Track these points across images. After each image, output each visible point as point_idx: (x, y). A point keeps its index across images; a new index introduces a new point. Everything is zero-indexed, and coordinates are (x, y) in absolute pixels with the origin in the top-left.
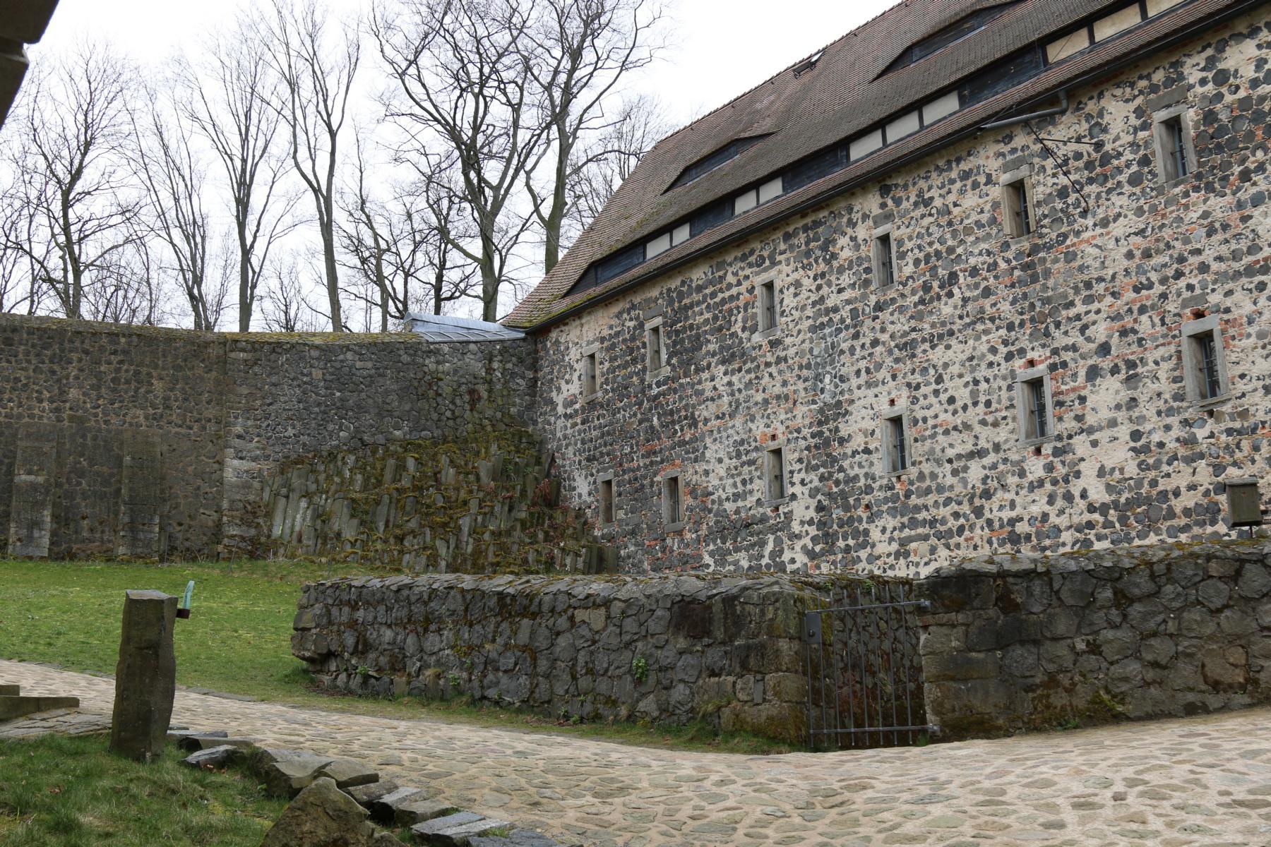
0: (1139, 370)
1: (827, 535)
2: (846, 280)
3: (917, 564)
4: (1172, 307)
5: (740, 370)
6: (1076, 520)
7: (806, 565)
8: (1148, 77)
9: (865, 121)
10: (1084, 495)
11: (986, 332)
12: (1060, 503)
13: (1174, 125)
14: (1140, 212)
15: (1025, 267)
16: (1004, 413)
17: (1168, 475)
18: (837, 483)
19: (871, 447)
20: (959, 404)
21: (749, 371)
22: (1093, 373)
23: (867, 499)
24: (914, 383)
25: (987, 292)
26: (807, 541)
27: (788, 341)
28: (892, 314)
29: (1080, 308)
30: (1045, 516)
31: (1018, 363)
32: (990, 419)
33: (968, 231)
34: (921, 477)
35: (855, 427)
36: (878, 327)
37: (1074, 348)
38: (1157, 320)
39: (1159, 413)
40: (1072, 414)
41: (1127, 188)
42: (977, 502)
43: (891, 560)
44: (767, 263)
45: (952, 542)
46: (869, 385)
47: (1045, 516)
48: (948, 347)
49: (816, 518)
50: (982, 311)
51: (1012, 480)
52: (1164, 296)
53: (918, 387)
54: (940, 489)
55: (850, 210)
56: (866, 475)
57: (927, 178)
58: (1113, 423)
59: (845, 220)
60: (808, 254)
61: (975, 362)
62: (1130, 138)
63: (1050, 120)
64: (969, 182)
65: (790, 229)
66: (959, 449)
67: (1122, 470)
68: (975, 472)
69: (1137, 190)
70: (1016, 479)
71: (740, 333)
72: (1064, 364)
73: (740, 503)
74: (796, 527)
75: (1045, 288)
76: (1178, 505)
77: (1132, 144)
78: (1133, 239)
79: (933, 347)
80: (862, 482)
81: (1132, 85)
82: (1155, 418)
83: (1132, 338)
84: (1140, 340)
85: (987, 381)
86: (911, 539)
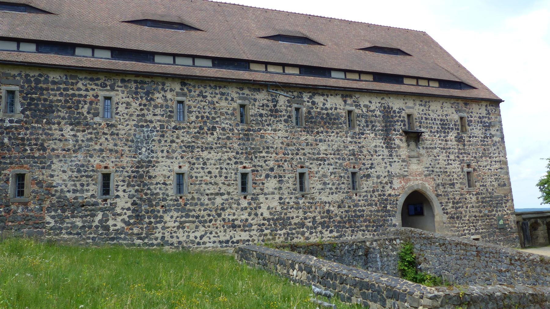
0: (283, 179)
1: (138, 216)
2: (158, 111)
3: (189, 232)
5: (84, 131)
6: (259, 222)
7: (123, 228)
9: (170, 51)
10: (262, 215)
11: (227, 152)
12: (252, 216)
14: (287, 131)
15: (245, 135)
16: (233, 182)
17: (290, 212)
18: (146, 194)
19: (168, 183)
20: (213, 175)
21: (91, 133)
22: (267, 176)
23: (163, 203)
24: (192, 162)
25: (228, 138)
26: (125, 217)
27: (119, 127)
28: (183, 133)
29: (264, 154)
30: (247, 220)
31: (240, 166)
32: (226, 183)
33: (222, 114)
34: (193, 198)
35: (160, 173)
36: (175, 136)
37: (261, 166)
38: (290, 165)
40: (259, 188)
42: (219, 212)
43: (175, 229)
44: (108, 88)
45: (206, 225)
46: (167, 157)
47: (247, 220)
48: (210, 153)
49: (132, 207)
50: (226, 144)
51: (235, 206)
52: (292, 159)
53: (194, 164)
54: (202, 204)
55: (164, 84)
56: (163, 194)
57: (205, 88)
58: (273, 193)
59: (160, 87)
60: (136, 93)
61: (221, 161)
62: (285, 108)
63: (259, 90)
64: (224, 97)
65: (127, 79)
66: (212, 191)
67: (276, 209)
68: (219, 200)
69: (287, 125)
70: (236, 206)
71: (85, 114)
72: (257, 171)
73: (78, 194)
74: (118, 210)
75: (251, 144)
76: (293, 221)
77: (286, 110)
79: (202, 151)
80: (161, 196)
82: (287, 194)
83: (281, 168)
85: (226, 169)
86: (186, 222)
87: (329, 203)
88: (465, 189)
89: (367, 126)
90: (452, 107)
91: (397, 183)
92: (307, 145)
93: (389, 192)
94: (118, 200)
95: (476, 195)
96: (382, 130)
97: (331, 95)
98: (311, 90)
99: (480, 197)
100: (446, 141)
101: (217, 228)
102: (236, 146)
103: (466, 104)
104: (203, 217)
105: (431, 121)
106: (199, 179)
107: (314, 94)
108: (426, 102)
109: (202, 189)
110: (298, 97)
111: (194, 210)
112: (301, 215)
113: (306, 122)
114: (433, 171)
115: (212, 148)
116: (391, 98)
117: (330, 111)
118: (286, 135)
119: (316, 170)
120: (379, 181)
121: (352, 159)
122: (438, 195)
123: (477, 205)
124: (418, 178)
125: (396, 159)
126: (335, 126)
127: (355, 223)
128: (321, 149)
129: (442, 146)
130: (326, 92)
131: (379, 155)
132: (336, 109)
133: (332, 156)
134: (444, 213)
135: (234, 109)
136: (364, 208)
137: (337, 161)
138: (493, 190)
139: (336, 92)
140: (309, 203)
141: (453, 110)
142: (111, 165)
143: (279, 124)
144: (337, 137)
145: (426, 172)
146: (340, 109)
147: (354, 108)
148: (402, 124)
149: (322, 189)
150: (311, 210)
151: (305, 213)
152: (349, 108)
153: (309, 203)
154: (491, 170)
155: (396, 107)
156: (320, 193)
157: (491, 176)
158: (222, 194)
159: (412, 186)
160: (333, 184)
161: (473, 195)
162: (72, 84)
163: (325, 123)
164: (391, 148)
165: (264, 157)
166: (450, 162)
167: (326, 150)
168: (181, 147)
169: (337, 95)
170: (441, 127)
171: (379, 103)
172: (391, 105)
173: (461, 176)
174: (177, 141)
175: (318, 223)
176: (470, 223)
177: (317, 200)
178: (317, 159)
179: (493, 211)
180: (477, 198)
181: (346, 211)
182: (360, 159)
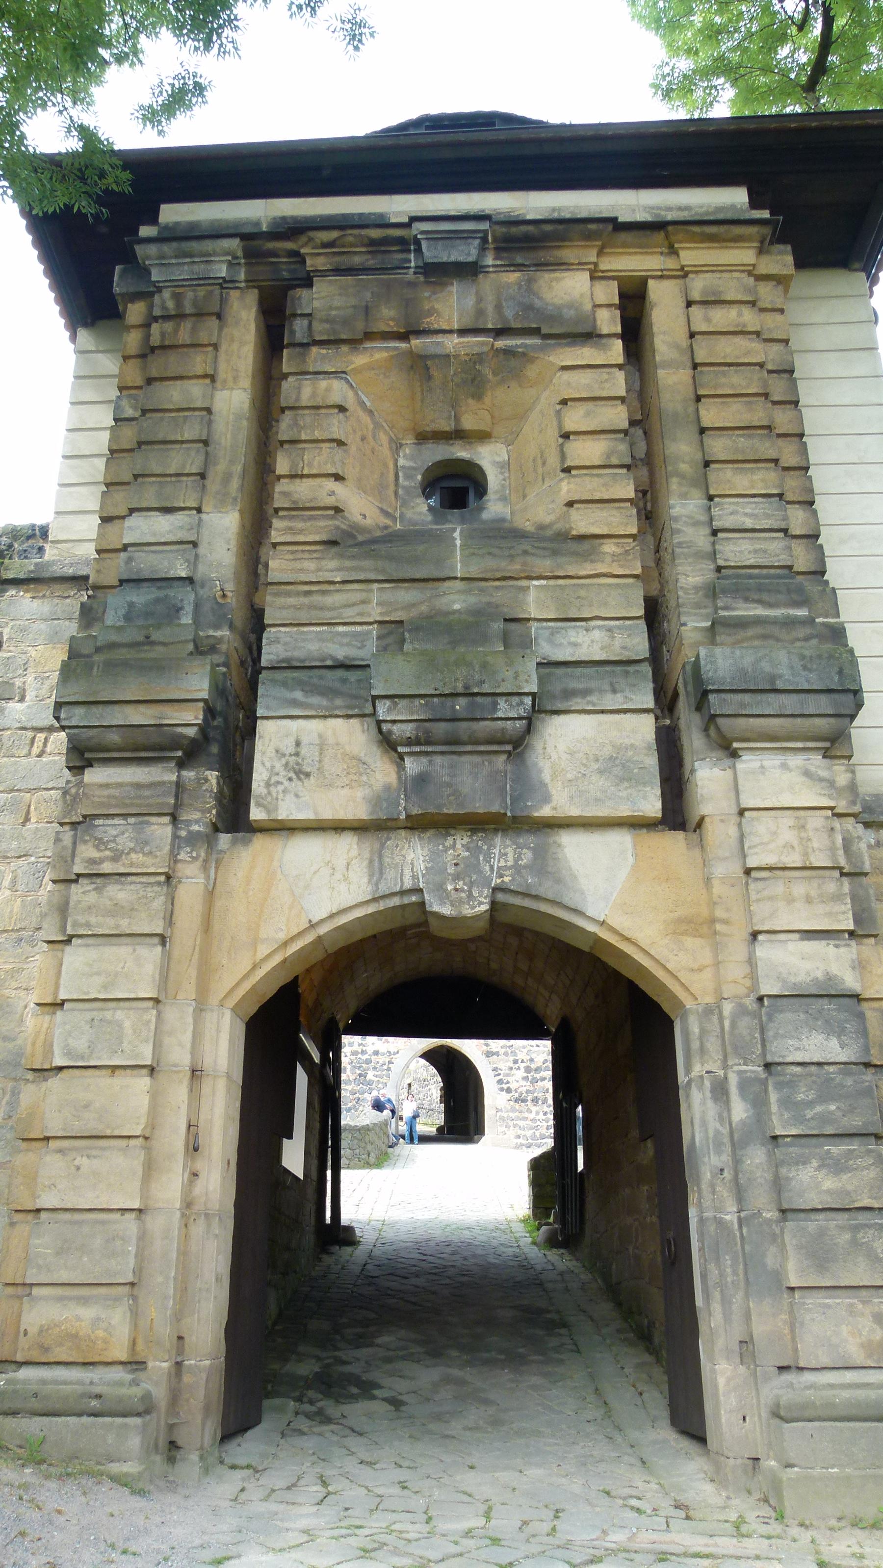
134: (502, 1090)
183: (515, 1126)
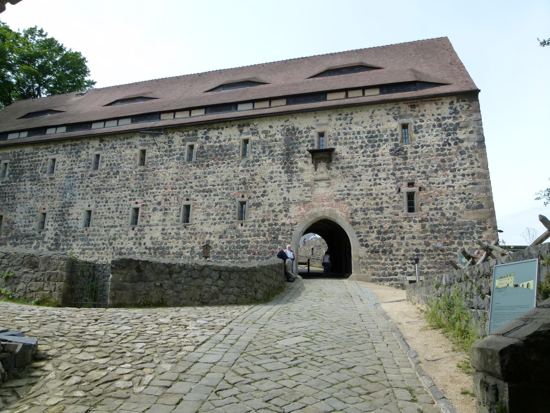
0: (168, 211)
1: (57, 243)
2: (82, 164)
4: (181, 196)
6: (141, 251)
8: (188, 132)
10: (145, 244)
11: (125, 191)
12: (137, 245)
13: (192, 147)
14: (177, 168)
15: (141, 175)
18: (64, 227)
19: (79, 218)
20: (111, 210)
21: (40, 186)
22: (155, 210)
23: (74, 234)
24: (98, 201)
27: (57, 179)
29: (154, 190)
30: (132, 248)
31: (133, 202)
32: (120, 217)
33: (125, 160)
34: (94, 230)
36: (90, 182)
37: (150, 201)
38: (176, 199)
39: (171, 224)
41: (175, 160)
42: (111, 241)
43: (78, 255)
44: (55, 152)
45: (100, 252)
46: (82, 199)
47: (132, 248)
48: (112, 193)
50: (125, 184)
51: (124, 236)
52: (179, 192)
53: (99, 203)
54: (100, 235)
55: (88, 143)
56: (75, 227)
57: (116, 141)
58: (157, 225)
59: (86, 146)
60: (70, 153)
62: (179, 147)
63: (158, 135)
64: (129, 146)
65: (66, 144)
66: (108, 224)
67: (157, 239)
68: (112, 231)
69: (178, 162)
70: (125, 236)
71: (39, 172)
72: (147, 205)
74: (46, 239)
75: (145, 182)
76: (171, 251)
77: (180, 149)
78: (174, 175)
79: (107, 192)
80: (73, 229)
81: (183, 133)
82: (170, 226)
83: (168, 202)
84: (170, 203)
86: (87, 249)
87: (210, 234)
88: (401, 215)
89: (264, 152)
90: (388, 114)
91: (294, 211)
92: (196, 178)
93: (283, 221)
94: (47, 232)
95: (420, 222)
96: (282, 154)
97: (227, 127)
98: (206, 126)
99: (428, 224)
100: (374, 156)
101: (107, 254)
102: (132, 185)
103: (413, 107)
104: (99, 245)
105: (352, 136)
106: (101, 214)
107: (209, 130)
108: (347, 115)
109: (102, 223)
110: (193, 135)
111: (94, 240)
112: (180, 243)
113: (197, 156)
114: (349, 194)
115: (113, 189)
116: (298, 118)
117: (223, 143)
118: (177, 171)
119: (201, 201)
120: (271, 209)
121: (241, 188)
122: (354, 224)
123: (422, 235)
124: (325, 203)
125: (296, 184)
126: (227, 157)
127: (236, 255)
128: (209, 181)
129: (367, 163)
130: (221, 125)
131: (275, 182)
132: (230, 139)
133: (220, 187)
134: (362, 245)
135: (136, 155)
136: (249, 239)
137: (225, 191)
138: (455, 214)
139: (232, 123)
140: (190, 233)
141: (390, 117)
142: (47, 207)
143: (171, 162)
144: (228, 167)
145: (338, 197)
146: (234, 139)
147: (251, 136)
148: (309, 144)
149: (205, 220)
150: (191, 240)
151: (184, 243)
152: (244, 137)
153: (190, 233)
154: (453, 187)
155: (302, 128)
156: (202, 224)
157: (454, 195)
158: (116, 227)
159: (316, 214)
160: (217, 215)
161: (415, 222)
162: (36, 153)
163: (217, 155)
164: (292, 172)
165: (153, 193)
166: (378, 181)
167: (214, 181)
168: (92, 190)
169: (232, 126)
170: (369, 141)
171: (282, 126)
172: (296, 126)
173: (396, 198)
174: (91, 185)
175: (196, 253)
176: (406, 258)
177: (199, 230)
178: (204, 191)
179: (452, 243)
180: (423, 227)
181: (229, 242)
182: (251, 187)
183: (371, 268)
